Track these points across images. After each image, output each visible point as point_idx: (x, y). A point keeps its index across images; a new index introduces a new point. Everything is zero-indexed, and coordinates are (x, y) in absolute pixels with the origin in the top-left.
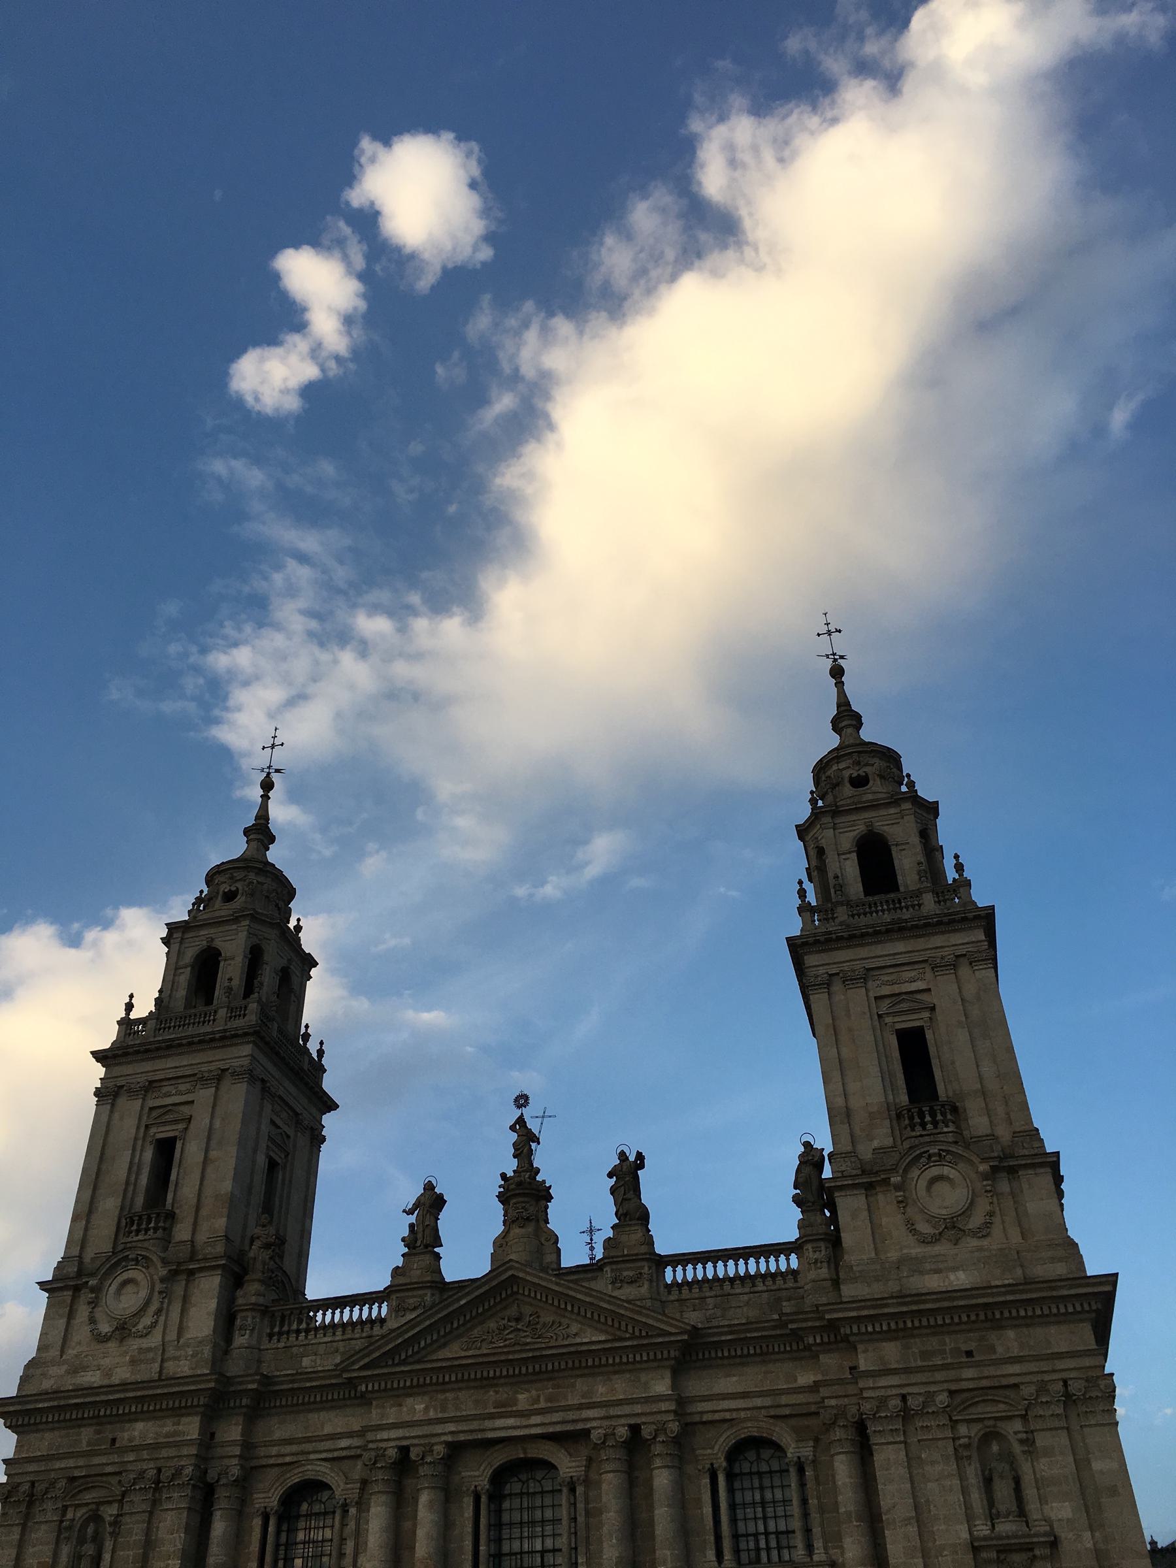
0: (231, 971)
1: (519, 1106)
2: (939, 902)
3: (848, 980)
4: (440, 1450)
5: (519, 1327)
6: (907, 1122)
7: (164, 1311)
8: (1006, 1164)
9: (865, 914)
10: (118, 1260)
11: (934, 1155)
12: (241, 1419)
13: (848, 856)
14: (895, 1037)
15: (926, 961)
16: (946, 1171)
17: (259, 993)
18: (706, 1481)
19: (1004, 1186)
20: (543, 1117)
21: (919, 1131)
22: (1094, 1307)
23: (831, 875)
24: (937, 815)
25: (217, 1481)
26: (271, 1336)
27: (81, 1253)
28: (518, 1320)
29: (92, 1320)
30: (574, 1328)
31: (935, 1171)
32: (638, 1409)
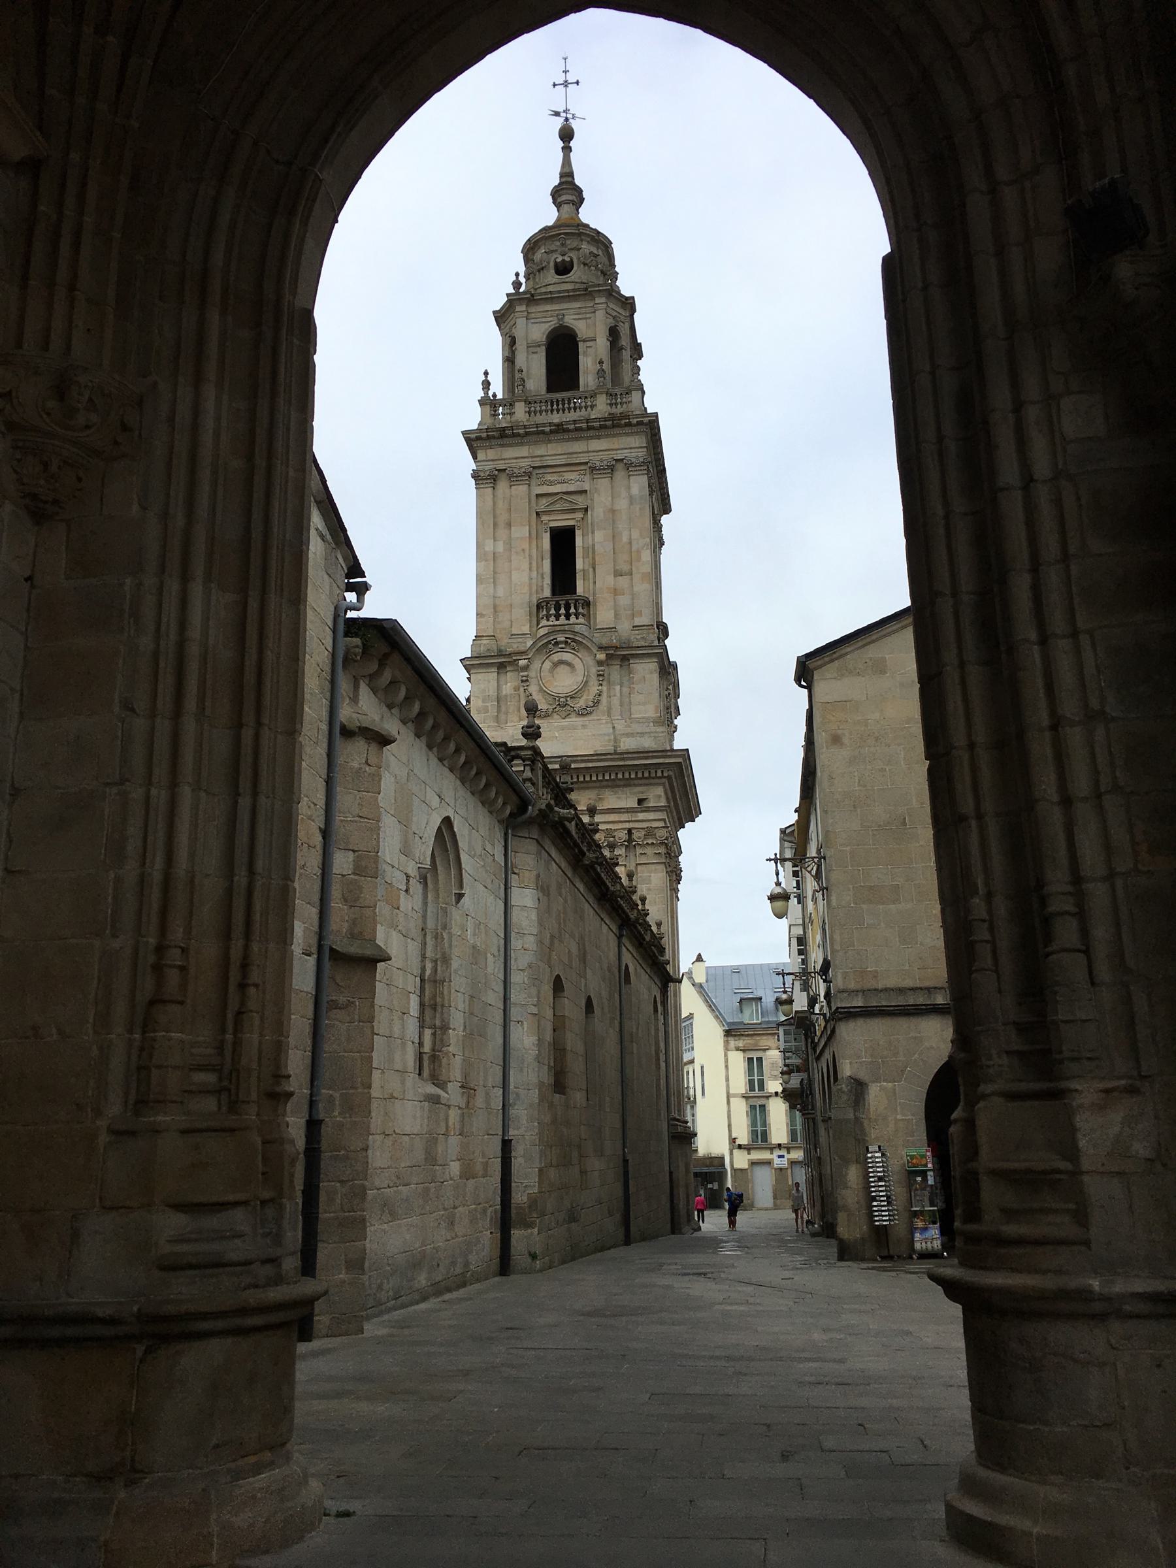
2: (611, 405)
3: (514, 477)
6: (545, 612)
8: (619, 653)
9: (541, 412)
11: (561, 642)
13: (538, 349)
14: (548, 534)
15: (587, 463)
16: (567, 657)
19: (615, 672)
21: (553, 620)
22: (665, 774)
23: (517, 368)
24: (633, 310)
31: (556, 657)
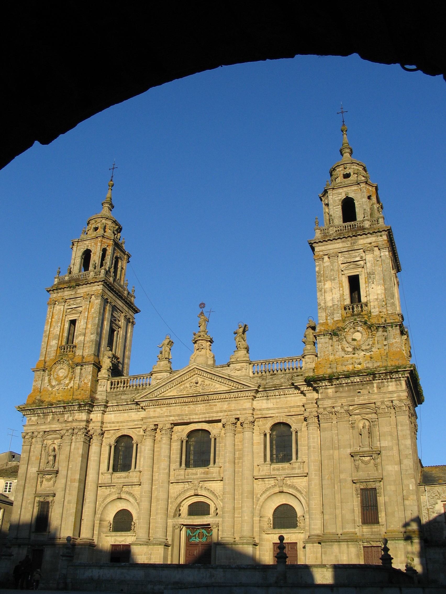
0: (95, 258)
1: (201, 308)
4: (169, 426)
5: (198, 386)
7: (73, 379)
10: (57, 362)
12: (101, 414)
17: (105, 266)
18: (262, 436)
20: (210, 312)
25: (93, 434)
26: (111, 388)
27: (45, 359)
28: (197, 383)
29: (50, 381)
30: (218, 386)
32: (239, 412)
